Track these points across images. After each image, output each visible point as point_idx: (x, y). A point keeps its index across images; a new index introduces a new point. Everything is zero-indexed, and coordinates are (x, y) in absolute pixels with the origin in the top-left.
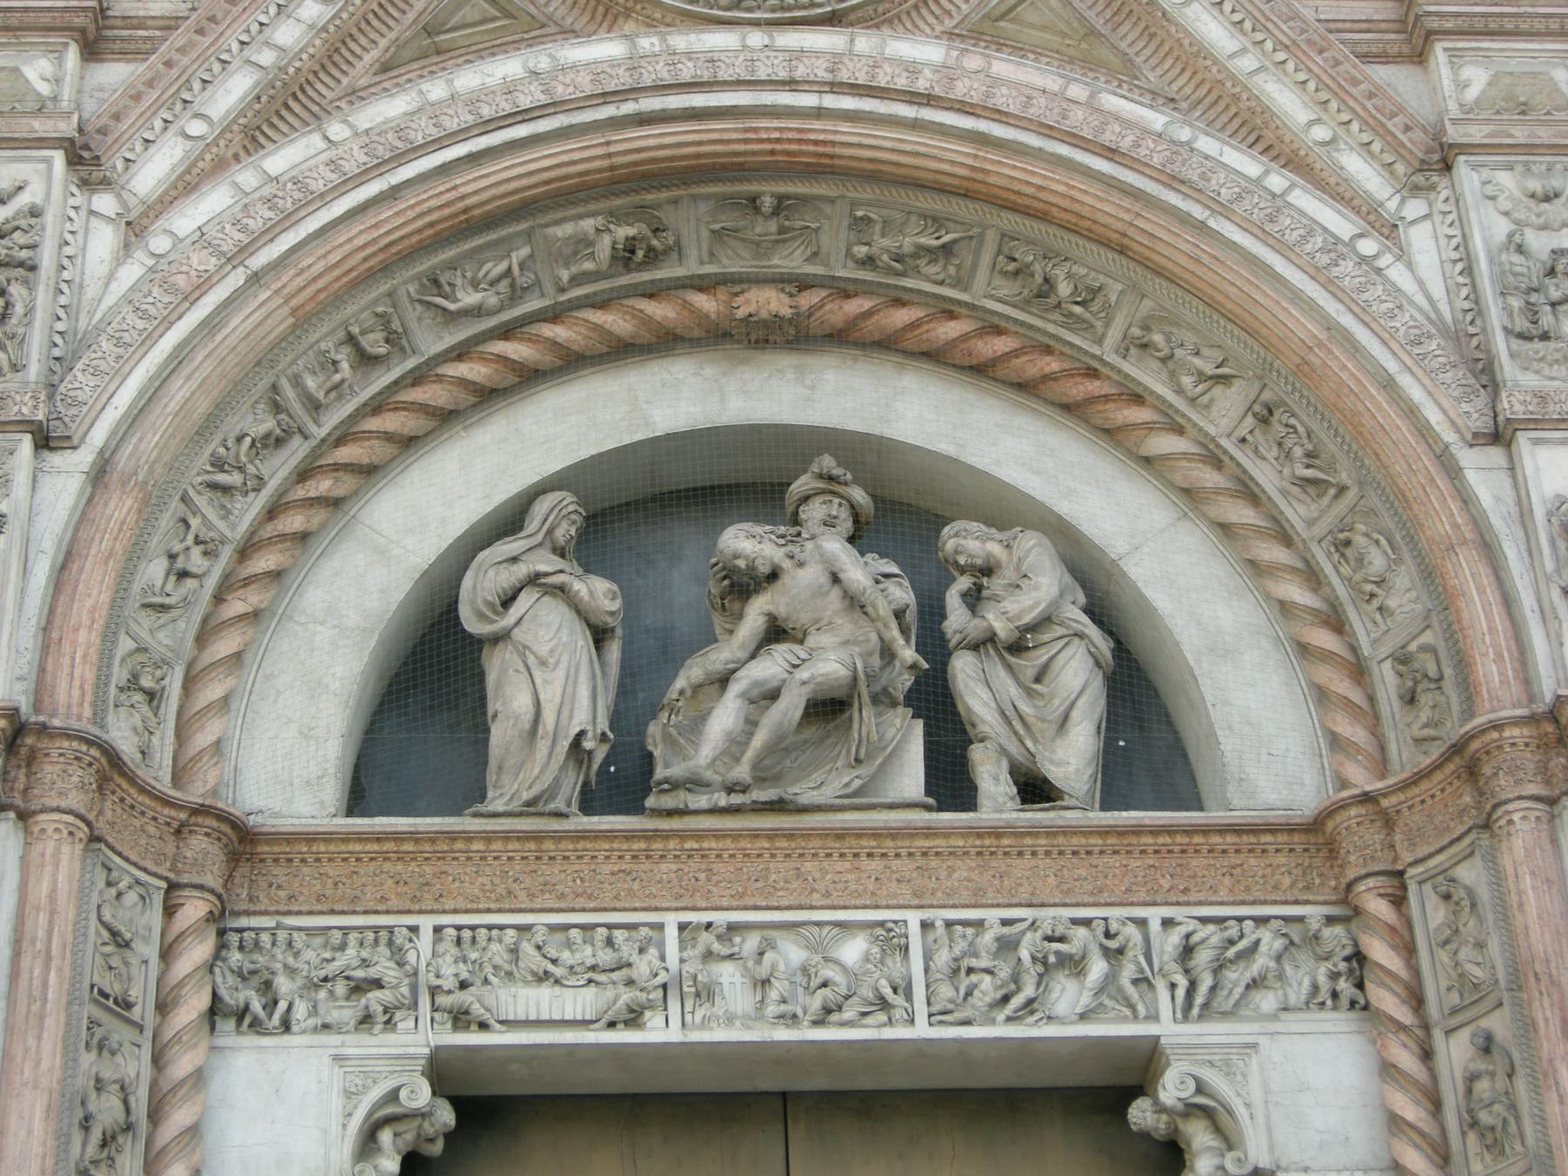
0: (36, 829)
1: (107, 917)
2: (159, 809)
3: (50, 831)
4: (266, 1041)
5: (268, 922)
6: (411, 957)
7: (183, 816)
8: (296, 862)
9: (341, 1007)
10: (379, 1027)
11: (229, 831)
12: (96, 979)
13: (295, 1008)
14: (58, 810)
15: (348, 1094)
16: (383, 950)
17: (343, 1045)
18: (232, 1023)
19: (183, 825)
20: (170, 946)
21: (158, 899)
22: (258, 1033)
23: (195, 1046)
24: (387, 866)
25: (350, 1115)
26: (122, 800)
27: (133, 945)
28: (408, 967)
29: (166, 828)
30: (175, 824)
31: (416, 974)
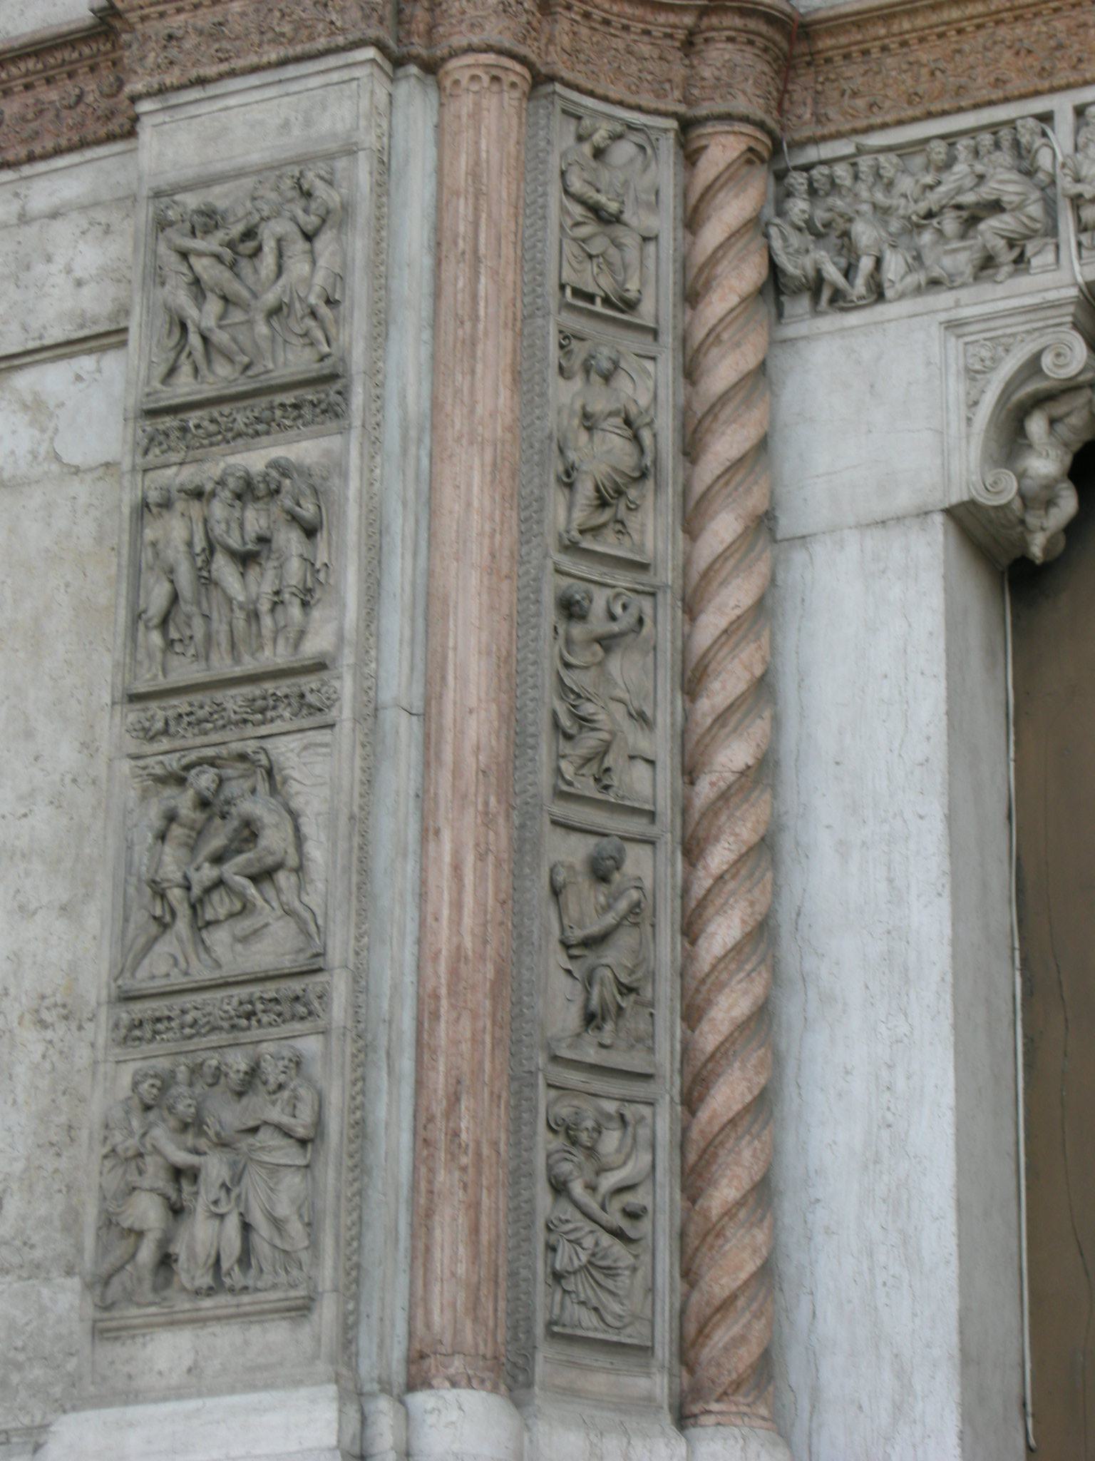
0: (448, 83)
1: (577, 185)
2: (650, 17)
3: (465, 82)
4: (853, 319)
5: (844, 148)
6: (1044, 159)
7: (688, 20)
8: (875, 53)
9: (955, 251)
10: (1006, 270)
11: (763, 28)
12: (568, 275)
13: (885, 265)
14: (471, 49)
15: (971, 374)
16: (1005, 157)
17: (958, 305)
18: (804, 302)
19: (692, 33)
20: (696, 209)
21: (668, 145)
22: (843, 310)
23: (738, 345)
24: (1003, 31)
25: (976, 403)
26: (587, 15)
27: (626, 217)
28: (1041, 176)
29: (669, 42)
30: (681, 34)
31: (1053, 183)
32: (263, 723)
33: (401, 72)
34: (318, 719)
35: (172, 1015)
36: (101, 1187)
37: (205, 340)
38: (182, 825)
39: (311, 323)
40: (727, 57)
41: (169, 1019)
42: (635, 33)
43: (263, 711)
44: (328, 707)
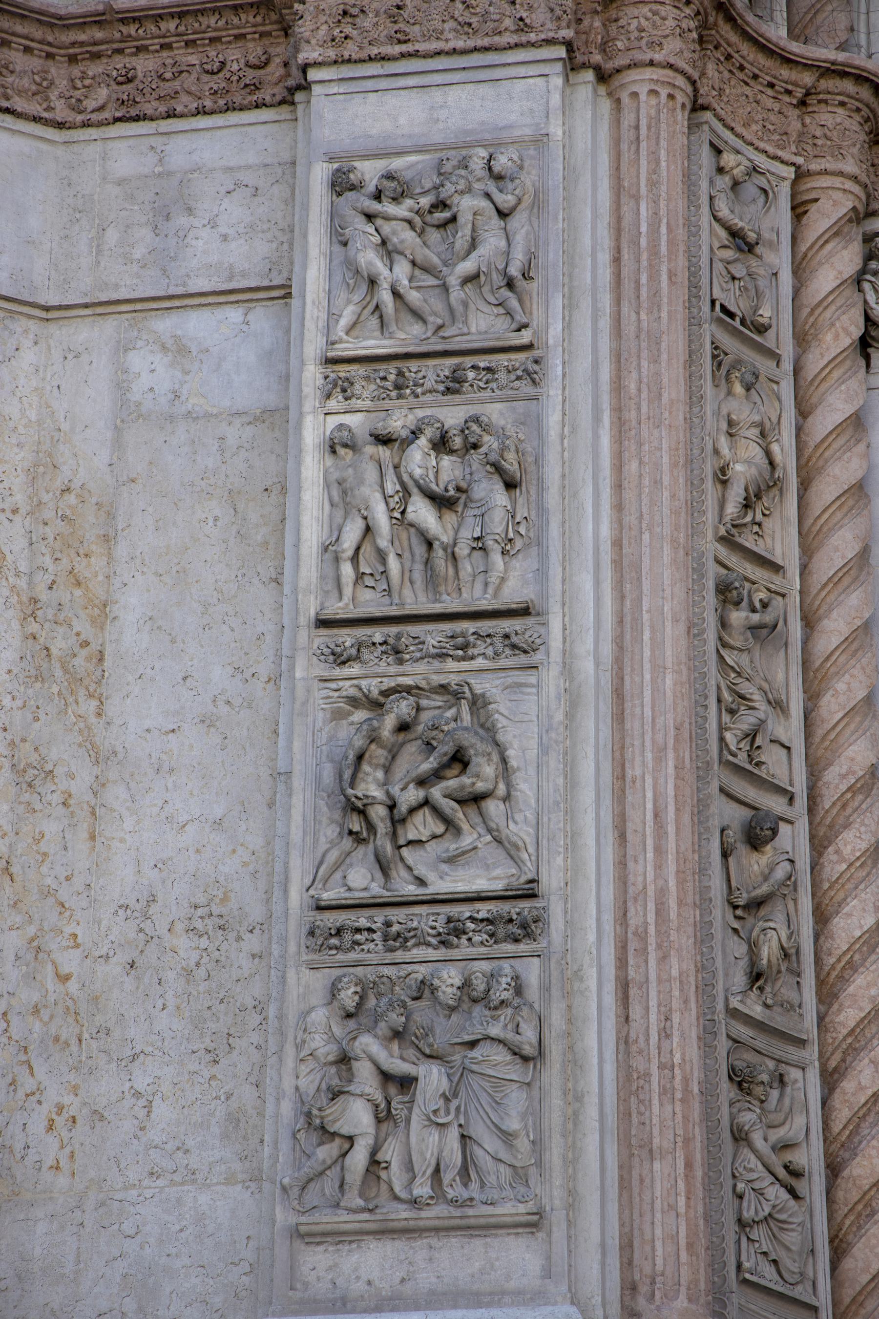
1: (724, 211)
27: (758, 250)
29: (787, 99)
30: (799, 93)
32: (463, 659)
33: (574, 78)
34: (523, 659)
35: (373, 926)
36: (297, 1088)
37: (396, 294)
38: (383, 747)
39: (505, 293)
40: (839, 120)
41: (370, 930)
42: (761, 84)
43: (464, 647)
44: (534, 651)
